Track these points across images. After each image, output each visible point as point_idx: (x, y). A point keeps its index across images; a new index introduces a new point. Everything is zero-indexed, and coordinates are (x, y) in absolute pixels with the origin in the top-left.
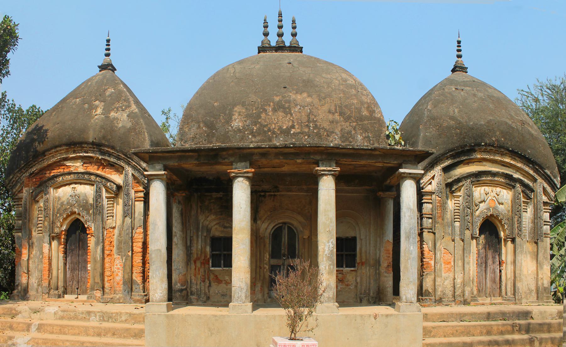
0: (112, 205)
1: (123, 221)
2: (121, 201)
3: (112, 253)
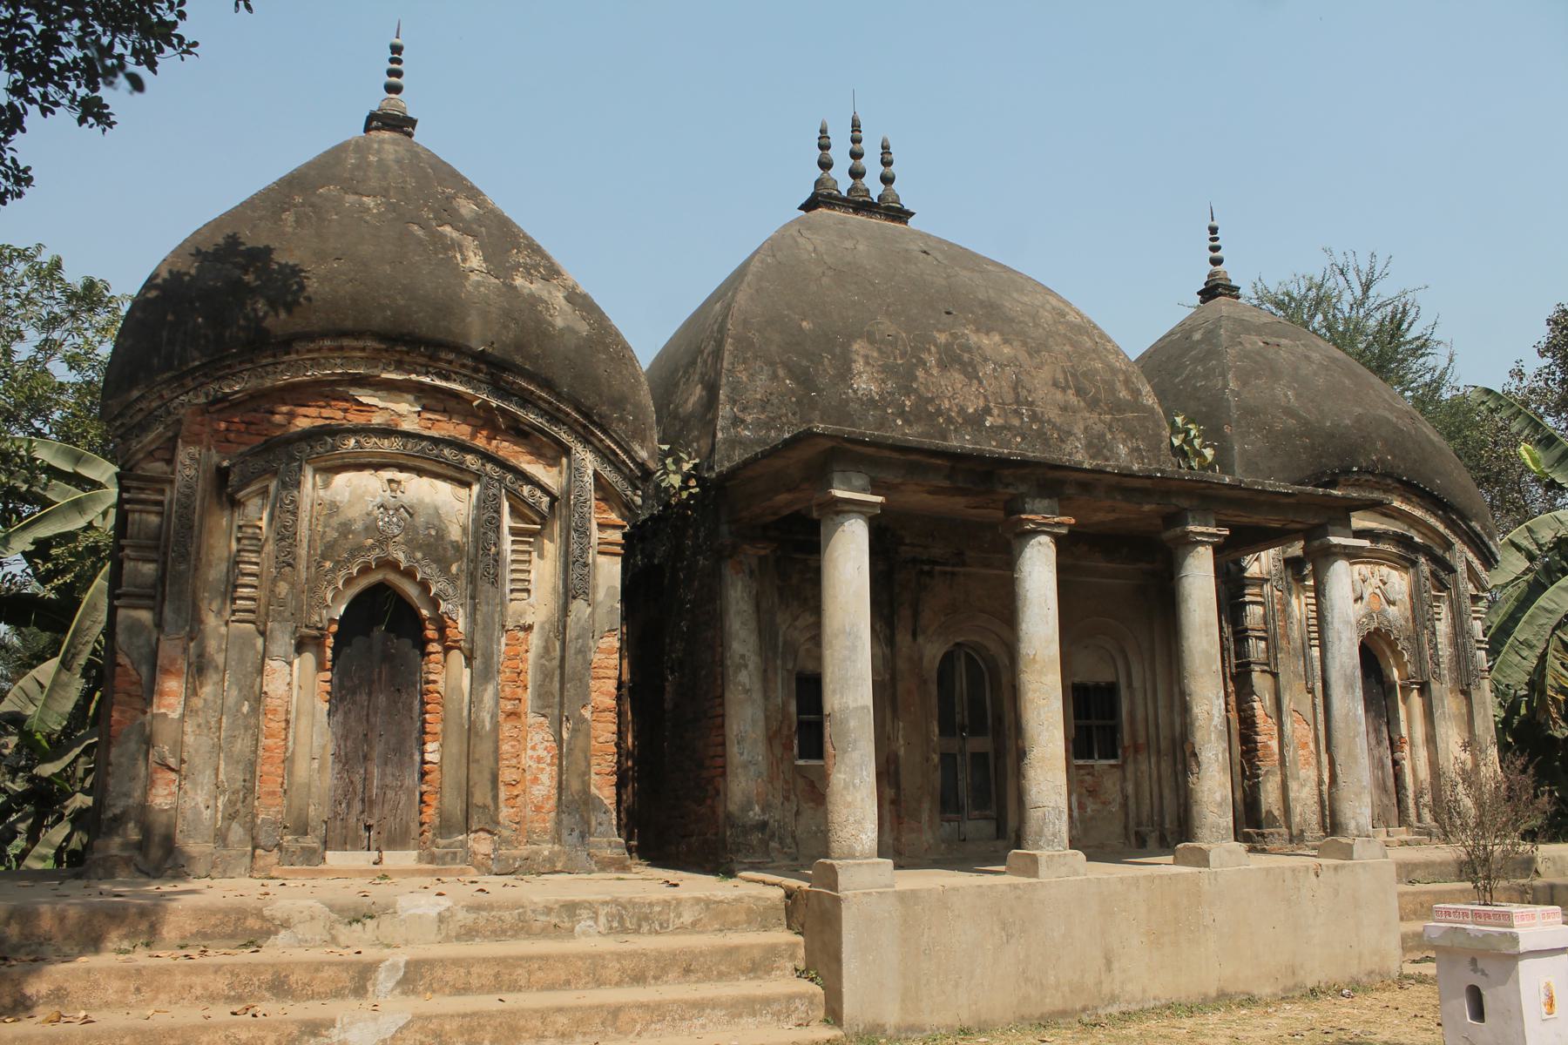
0: (525, 557)
1: (565, 610)
2: (551, 548)
3: (521, 709)
